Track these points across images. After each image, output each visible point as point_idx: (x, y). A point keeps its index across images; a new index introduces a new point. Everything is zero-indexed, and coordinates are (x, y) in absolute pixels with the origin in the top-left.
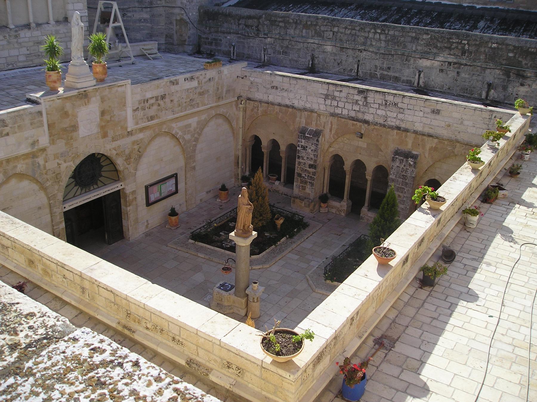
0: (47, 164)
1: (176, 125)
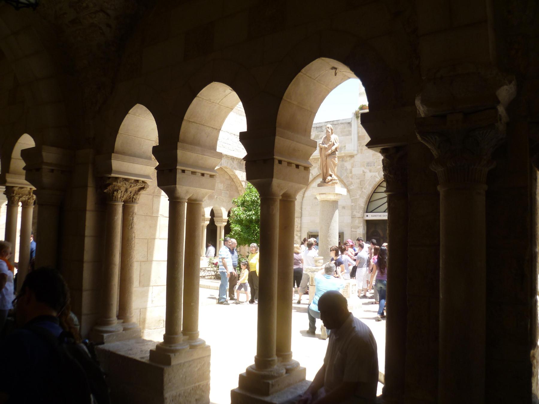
0: (353, 169)
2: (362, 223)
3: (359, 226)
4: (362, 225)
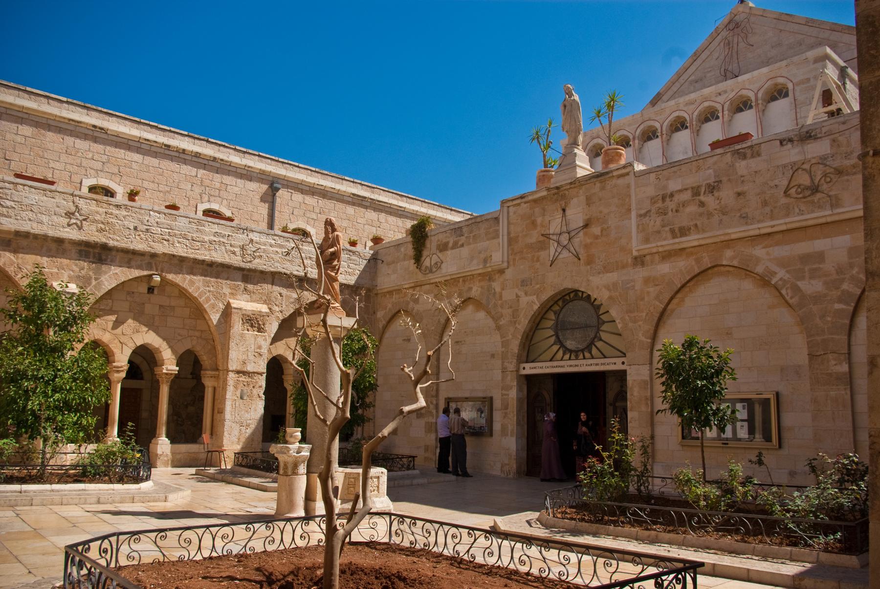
0: (503, 292)
1: (768, 254)
4: (515, 383)
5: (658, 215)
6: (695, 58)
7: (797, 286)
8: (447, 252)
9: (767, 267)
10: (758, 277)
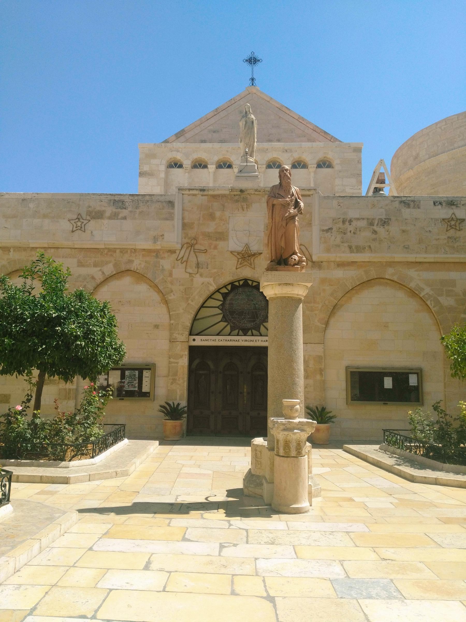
0: (174, 270)
2: (187, 350)
3: (183, 355)
5: (338, 233)
6: (216, 113)
7: (438, 299)
8: (102, 221)
9: (418, 284)
10: (409, 290)
